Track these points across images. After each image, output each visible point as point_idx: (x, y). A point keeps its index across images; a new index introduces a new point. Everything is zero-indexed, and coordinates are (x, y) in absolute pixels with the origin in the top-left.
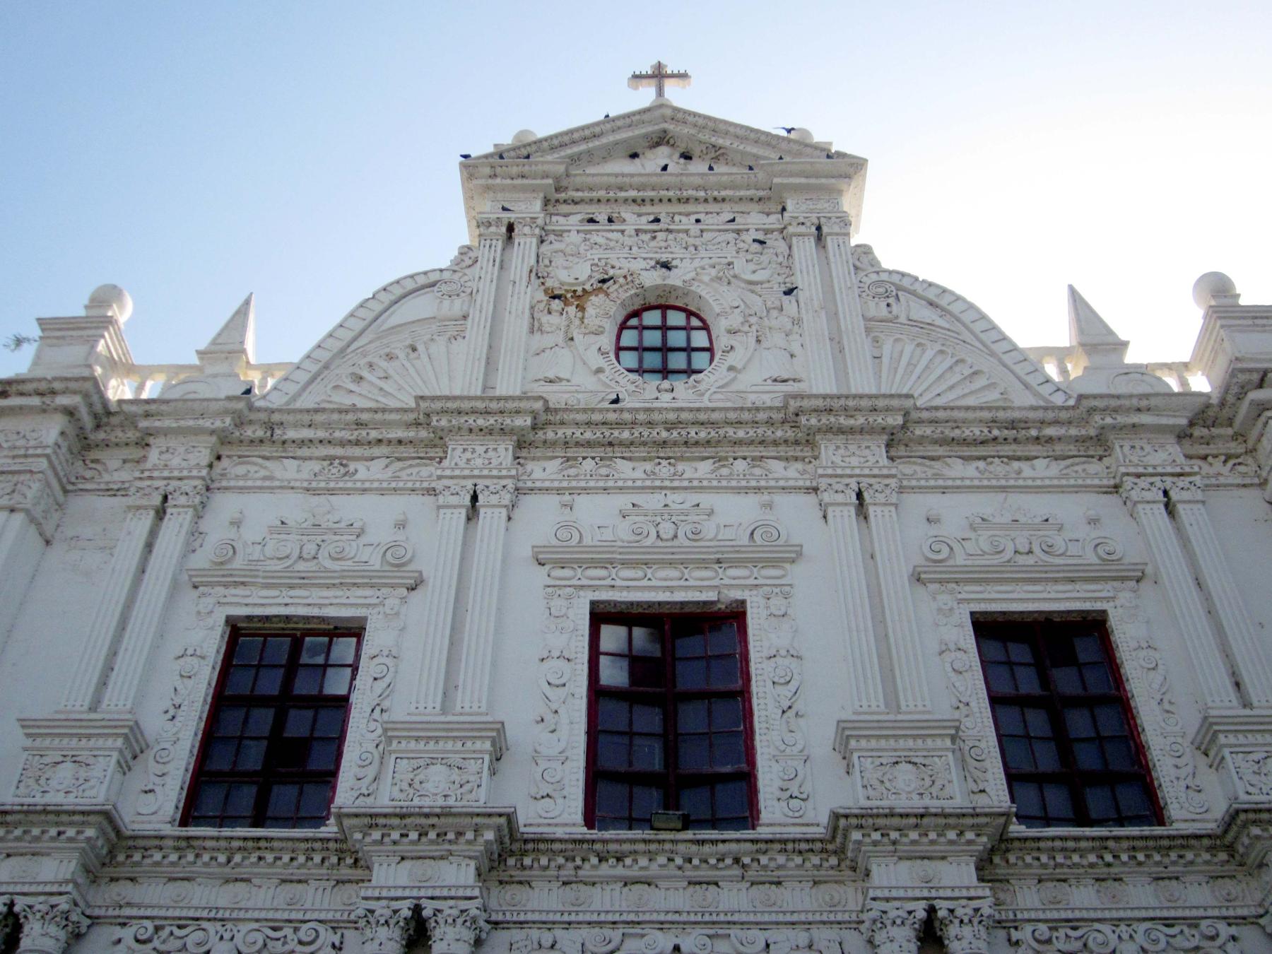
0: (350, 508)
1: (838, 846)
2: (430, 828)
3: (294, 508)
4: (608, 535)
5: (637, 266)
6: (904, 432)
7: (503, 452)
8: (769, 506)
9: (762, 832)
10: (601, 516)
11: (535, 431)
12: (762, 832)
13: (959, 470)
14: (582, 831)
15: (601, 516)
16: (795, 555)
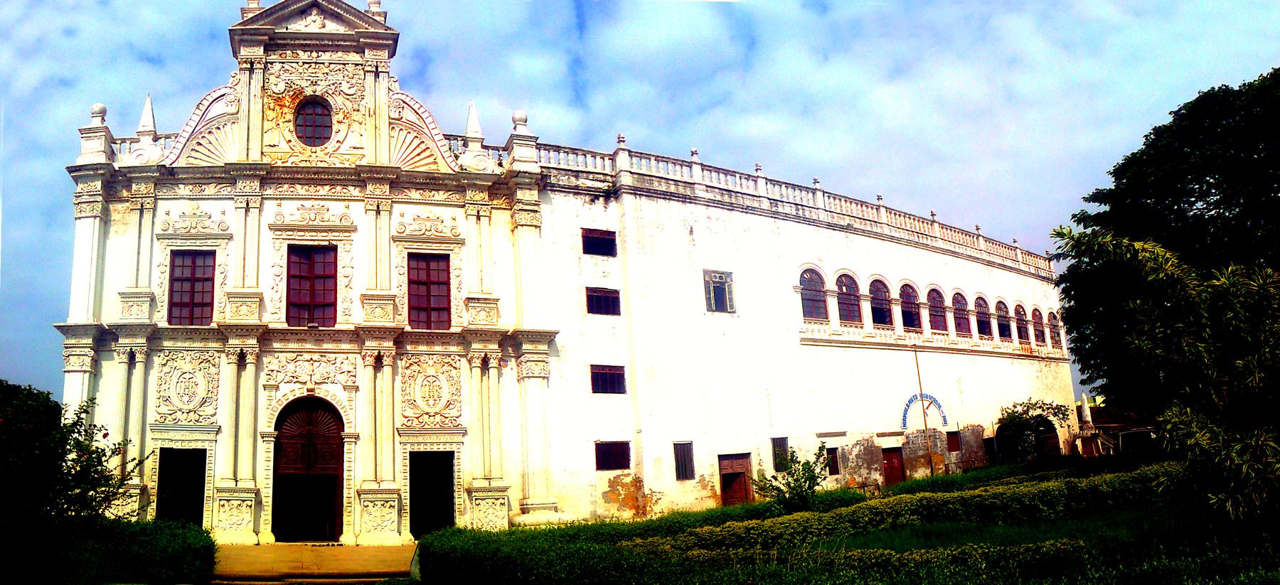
0: (206, 206)
1: (358, 335)
2: (244, 331)
3: (188, 206)
4: (293, 218)
5: (304, 84)
6: (398, 181)
7: (257, 184)
8: (348, 207)
9: (337, 327)
10: (291, 211)
11: (268, 176)
12: (337, 327)
13: (415, 195)
14: (285, 326)
15: (291, 211)
16: (352, 229)
